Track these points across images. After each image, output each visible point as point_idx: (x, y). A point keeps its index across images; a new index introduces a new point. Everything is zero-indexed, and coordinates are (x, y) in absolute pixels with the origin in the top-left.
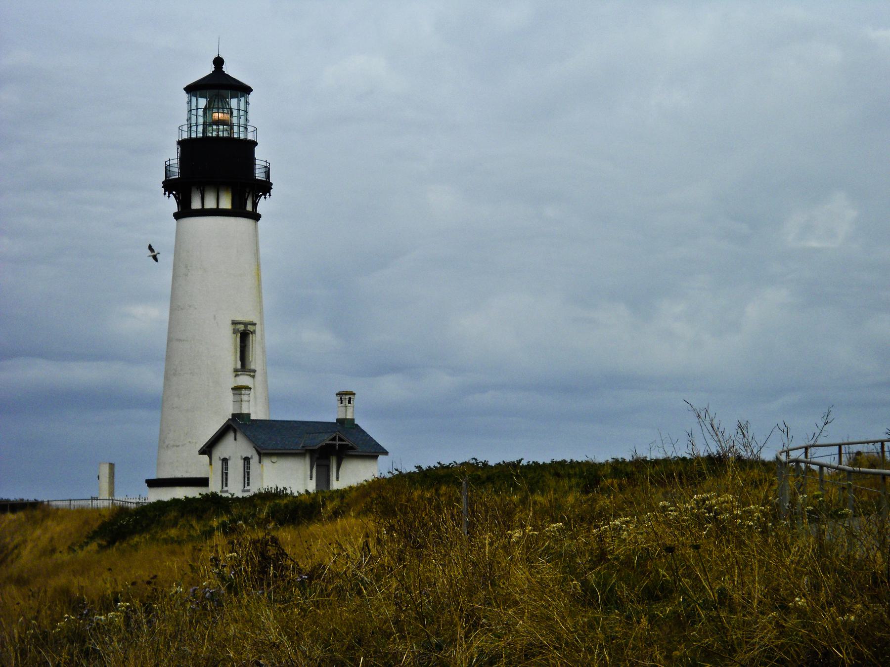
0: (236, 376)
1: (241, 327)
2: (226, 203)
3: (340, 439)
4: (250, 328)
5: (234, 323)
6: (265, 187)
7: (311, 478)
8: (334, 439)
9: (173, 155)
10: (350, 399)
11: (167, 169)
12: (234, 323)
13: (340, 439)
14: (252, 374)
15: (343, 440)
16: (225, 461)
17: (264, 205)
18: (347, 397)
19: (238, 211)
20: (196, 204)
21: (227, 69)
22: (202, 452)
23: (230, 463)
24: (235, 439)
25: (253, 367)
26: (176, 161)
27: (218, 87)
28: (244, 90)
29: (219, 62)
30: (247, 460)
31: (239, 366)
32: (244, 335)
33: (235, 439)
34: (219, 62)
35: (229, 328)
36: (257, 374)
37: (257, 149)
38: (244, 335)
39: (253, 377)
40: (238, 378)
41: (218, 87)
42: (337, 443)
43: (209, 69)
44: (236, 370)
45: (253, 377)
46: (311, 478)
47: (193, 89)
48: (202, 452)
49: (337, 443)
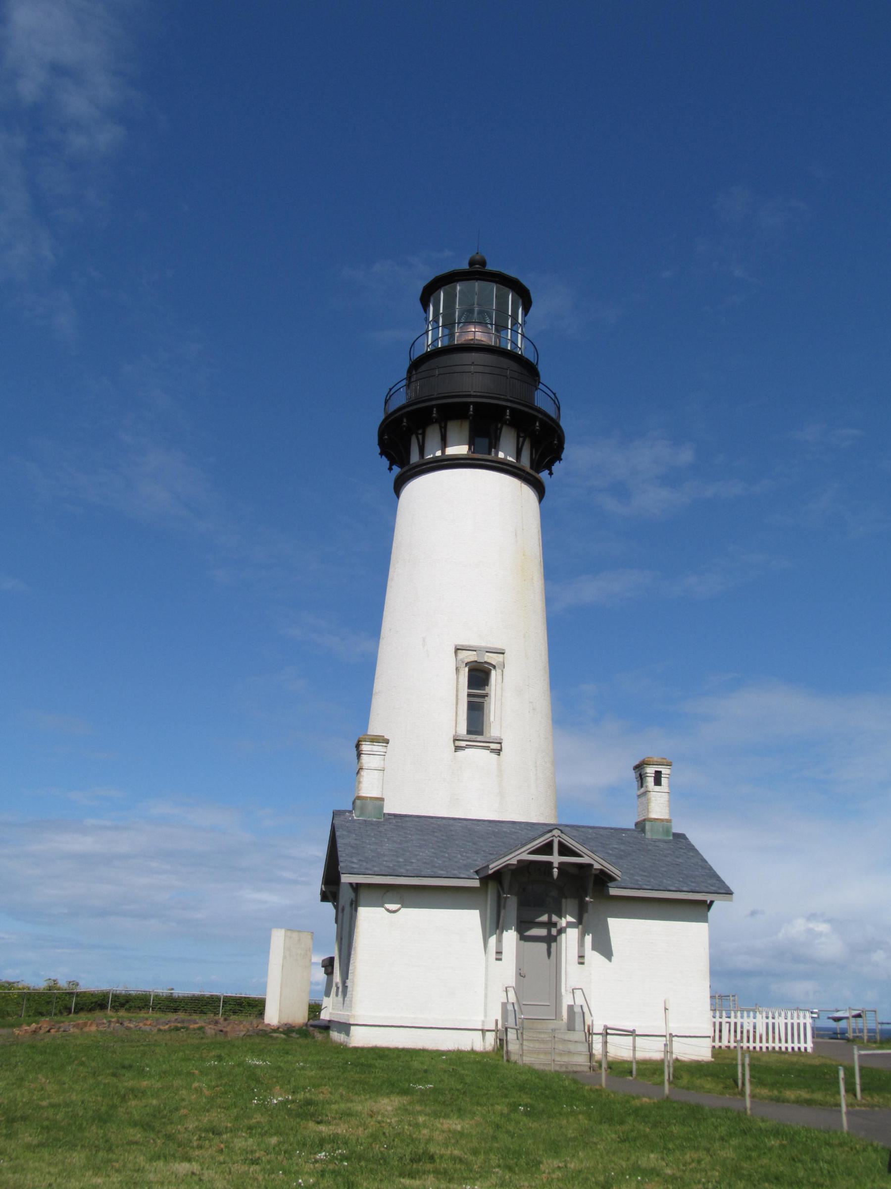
0: (457, 748)
1: (471, 656)
5: (457, 650)
8: (547, 849)
12: (457, 650)
13: (565, 850)
14: (493, 746)
31: (463, 729)
32: (479, 676)
39: (498, 752)
40: (460, 753)
44: (455, 740)
45: (498, 752)
46: (499, 953)
48: (324, 898)
49: (556, 859)
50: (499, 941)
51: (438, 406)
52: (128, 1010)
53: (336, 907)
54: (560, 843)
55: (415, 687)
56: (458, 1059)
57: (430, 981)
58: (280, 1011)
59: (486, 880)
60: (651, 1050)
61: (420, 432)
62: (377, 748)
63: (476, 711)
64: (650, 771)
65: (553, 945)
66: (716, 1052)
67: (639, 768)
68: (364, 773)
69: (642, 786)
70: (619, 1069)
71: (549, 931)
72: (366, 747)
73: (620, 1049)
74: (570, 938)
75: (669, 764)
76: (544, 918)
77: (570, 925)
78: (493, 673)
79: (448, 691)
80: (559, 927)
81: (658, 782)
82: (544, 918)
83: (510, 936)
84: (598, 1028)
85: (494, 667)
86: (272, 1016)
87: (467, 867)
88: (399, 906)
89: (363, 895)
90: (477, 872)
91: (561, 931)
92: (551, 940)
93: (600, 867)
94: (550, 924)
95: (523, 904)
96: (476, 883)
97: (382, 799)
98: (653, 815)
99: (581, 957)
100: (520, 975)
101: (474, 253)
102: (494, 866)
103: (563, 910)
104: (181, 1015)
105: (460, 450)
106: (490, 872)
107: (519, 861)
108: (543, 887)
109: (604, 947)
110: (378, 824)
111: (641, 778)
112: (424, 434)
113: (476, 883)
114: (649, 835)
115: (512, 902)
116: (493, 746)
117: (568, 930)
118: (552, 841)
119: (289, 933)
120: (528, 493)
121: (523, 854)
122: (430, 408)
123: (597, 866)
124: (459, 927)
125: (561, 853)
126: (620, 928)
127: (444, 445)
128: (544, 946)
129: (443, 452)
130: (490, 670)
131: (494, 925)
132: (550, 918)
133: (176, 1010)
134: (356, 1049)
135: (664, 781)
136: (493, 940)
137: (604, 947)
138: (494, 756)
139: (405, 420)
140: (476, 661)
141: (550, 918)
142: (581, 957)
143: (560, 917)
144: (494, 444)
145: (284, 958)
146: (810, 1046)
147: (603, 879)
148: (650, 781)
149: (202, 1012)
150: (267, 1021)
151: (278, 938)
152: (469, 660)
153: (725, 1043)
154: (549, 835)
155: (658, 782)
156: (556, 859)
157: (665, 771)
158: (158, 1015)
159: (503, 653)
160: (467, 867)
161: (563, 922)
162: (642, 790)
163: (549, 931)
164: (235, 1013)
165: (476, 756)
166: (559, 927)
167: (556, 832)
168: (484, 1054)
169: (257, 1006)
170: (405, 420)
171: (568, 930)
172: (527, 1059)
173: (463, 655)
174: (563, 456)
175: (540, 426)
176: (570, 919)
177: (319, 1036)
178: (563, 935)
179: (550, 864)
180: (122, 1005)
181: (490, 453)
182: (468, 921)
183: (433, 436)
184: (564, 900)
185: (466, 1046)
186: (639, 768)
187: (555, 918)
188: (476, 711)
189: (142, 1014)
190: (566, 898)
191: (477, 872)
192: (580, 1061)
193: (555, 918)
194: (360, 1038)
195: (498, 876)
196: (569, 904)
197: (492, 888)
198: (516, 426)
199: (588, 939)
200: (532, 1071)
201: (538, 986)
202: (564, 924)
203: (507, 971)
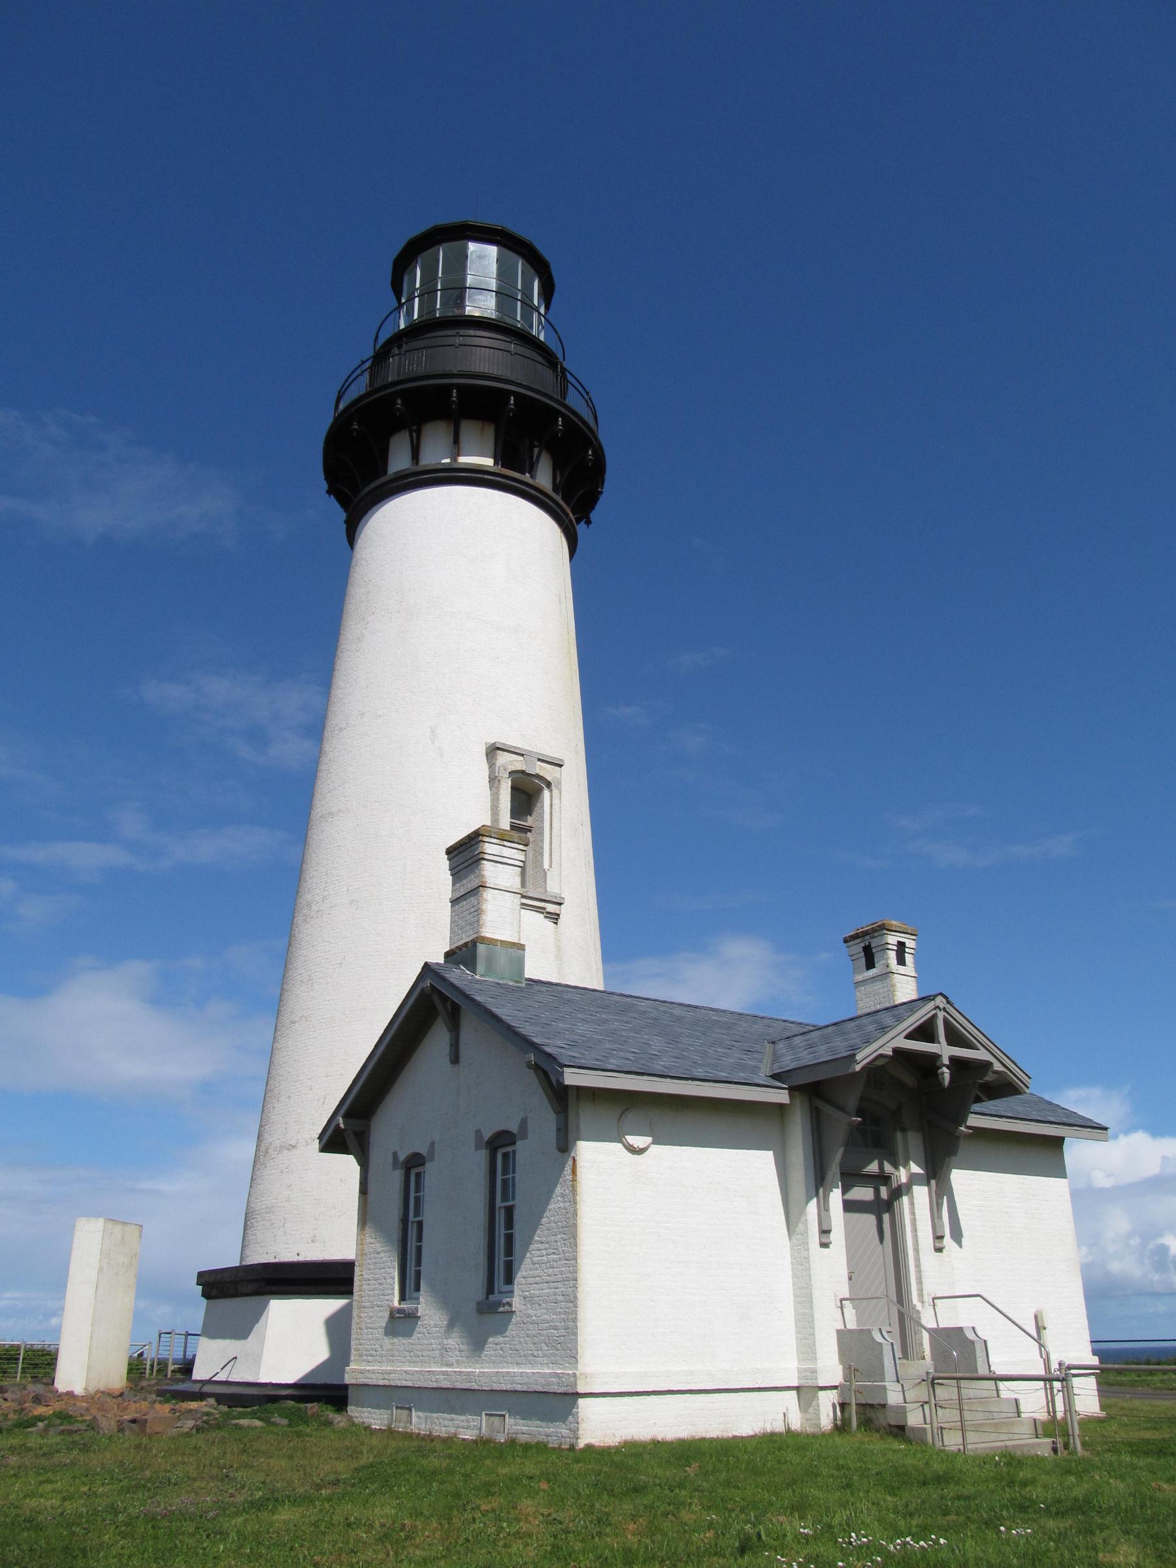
3: (955, 1038)
5: (493, 751)
7: (825, 1232)
8: (925, 1032)
10: (901, 945)
12: (493, 751)
14: (551, 908)
16: (413, 1164)
18: (892, 939)
22: (333, 1141)
23: (432, 1173)
24: (455, 1059)
25: (553, 887)
30: (500, 1146)
33: (455, 1059)
36: (564, 911)
39: (555, 918)
45: (555, 918)
46: (825, 1232)
48: (333, 1141)
50: (824, 1208)
51: (459, 387)
54: (947, 1023)
58: (89, 1368)
65: (886, 1217)
68: (488, 895)
69: (870, 964)
71: (877, 1192)
76: (873, 1167)
77: (913, 1179)
78: (546, 793)
80: (894, 1185)
81: (901, 961)
82: (873, 1167)
85: (549, 785)
86: (73, 1376)
88: (650, 1139)
90: (775, 1077)
91: (898, 1193)
92: (884, 1207)
93: (1002, 1069)
94: (883, 1179)
96: (781, 1097)
97: (521, 947)
103: (900, 1150)
106: (858, 1068)
107: (895, 1050)
112: (419, 432)
113: (781, 1097)
116: (551, 908)
117: (916, 1188)
118: (934, 1016)
119: (110, 1225)
121: (896, 1040)
122: (448, 389)
123: (997, 1066)
124: (740, 1181)
125: (951, 1043)
127: (456, 447)
128: (870, 1219)
129: (454, 459)
130: (540, 790)
132: (881, 1167)
135: (909, 958)
136: (812, 1206)
138: (549, 924)
139: (399, 401)
140: (523, 772)
141: (881, 1167)
143: (896, 1166)
145: (101, 1270)
148: (892, 955)
152: (514, 768)
154: (931, 1005)
155: (901, 961)
156: (945, 1050)
157: (910, 943)
159: (561, 766)
161: (902, 1176)
162: (872, 972)
163: (877, 1192)
166: (894, 1185)
167: (940, 1001)
169: (43, 1362)
170: (399, 401)
171: (916, 1188)
174: (594, 515)
175: (593, 455)
176: (915, 1169)
178: (905, 1199)
179: (936, 1057)
184: (899, 1135)
187: (888, 1168)
190: (904, 1130)
191: (775, 1077)
193: (888, 1168)
194: (601, 1424)
196: (913, 1141)
198: (550, 450)
202: (904, 1179)
203: (832, 1268)
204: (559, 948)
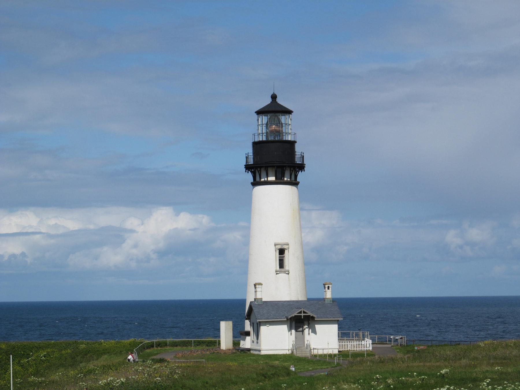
0: (277, 274)
1: (279, 247)
2: (272, 178)
4: (285, 247)
6: (301, 167)
8: (300, 312)
9: (250, 151)
11: (247, 158)
12: (275, 245)
13: (304, 312)
15: (306, 313)
16: (253, 324)
17: (301, 176)
18: (327, 286)
19: (279, 181)
20: (258, 179)
21: (280, 101)
26: (252, 154)
27: (274, 110)
28: (289, 112)
29: (274, 97)
32: (282, 252)
34: (274, 97)
35: (273, 248)
37: (296, 145)
38: (282, 252)
39: (288, 274)
41: (274, 110)
42: (302, 314)
43: (269, 101)
45: (288, 274)
47: (259, 113)
52: (161, 347)
53: (250, 321)
55: (263, 260)
56: (285, 356)
57: (275, 340)
59: (287, 319)
60: (325, 352)
61: (259, 169)
62: (260, 286)
63: (281, 264)
64: (327, 286)
66: (339, 351)
67: (324, 285)
70: (315, 356)
72: (257, 286)
73: (315, 352)
74: (306, 331)
75: (331, 284)
79: (273, 257)
81: (328, 288)
83: (293, 331)
84: (312, 348)
87: (283, 316)
89: (261, 324)
95: (296, 323)
98: (327, 297)
99: (309, 333)
100: (296, 338)
101: (272, 93)
102: (289, 317)
104: (179, 348)
105: (272, 178)
108: (300, 319)
109: (314, 332)
110: (261, 305)
111: (325, 288)
112: (260, 171)
114: (326, 302)
115: (294, 323)
120: (294, 188)
126: (318, 327)
131: (290, 329)
133: (177, 346)
134: (262, 355)
137: (314, 332)
142: (309, 333)
144: (283, 176)
146: (371, 348)
147: (313, 318)
148: (327, 288)
149: (186, 346)
150: (222, 348)
151: (223, 324)
153: (349, 349)
155: (328, 288)
156: (302, 314)
157: (330, 286)
158: (171, 348)
160: (283, 316)
164: (198, 345)
165: (282, 275)
168: (289, 354)
172: (298, 355)
173: (277, 246)
176: (306, 326)
177: (249, 353)
179: (301, 316)
180: (159, 345)
181: (281, 179)
182: (285, 327)
183: (263, 173)
185: (285, 353)
186: (324, 285)
188: (281, 264)
189: (166, 348)
192: (308, 355)
194: (263, 353)
195: (291, 318)
197: (289, 322)
199: (310, 330)
200: (298, 357)
201: (300, 342)
204: (289, 279)
